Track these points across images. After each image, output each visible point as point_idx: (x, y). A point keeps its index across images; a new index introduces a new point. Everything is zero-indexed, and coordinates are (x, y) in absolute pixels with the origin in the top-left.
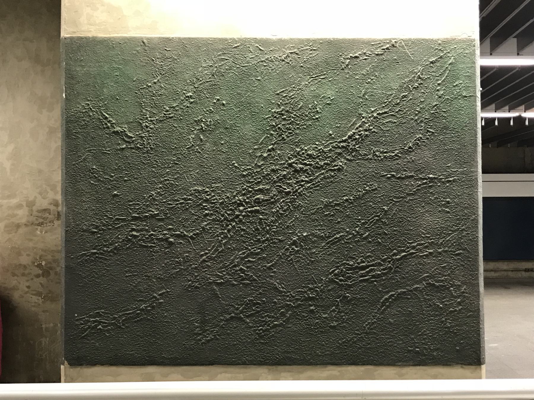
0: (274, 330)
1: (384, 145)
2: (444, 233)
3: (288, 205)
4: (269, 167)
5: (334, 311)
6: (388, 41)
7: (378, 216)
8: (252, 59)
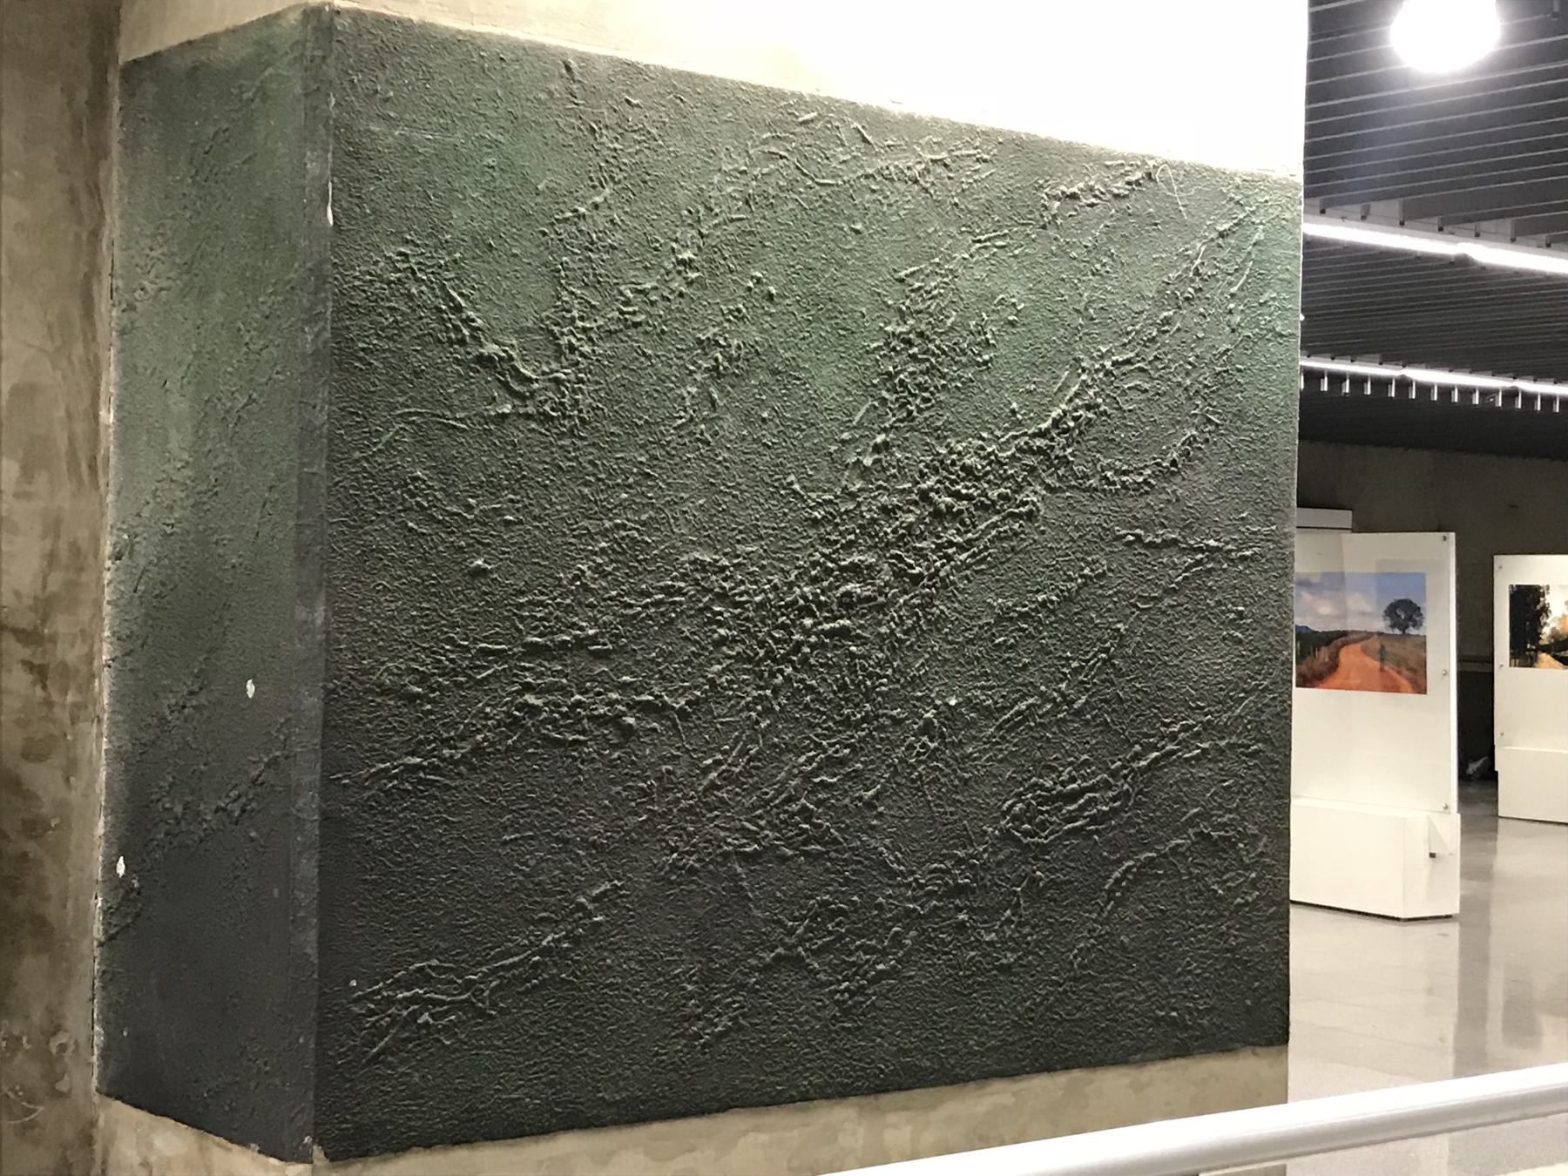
0: (876, 988)
4: (875, 498)
5: (1009, 921)
7: (1106, 651)
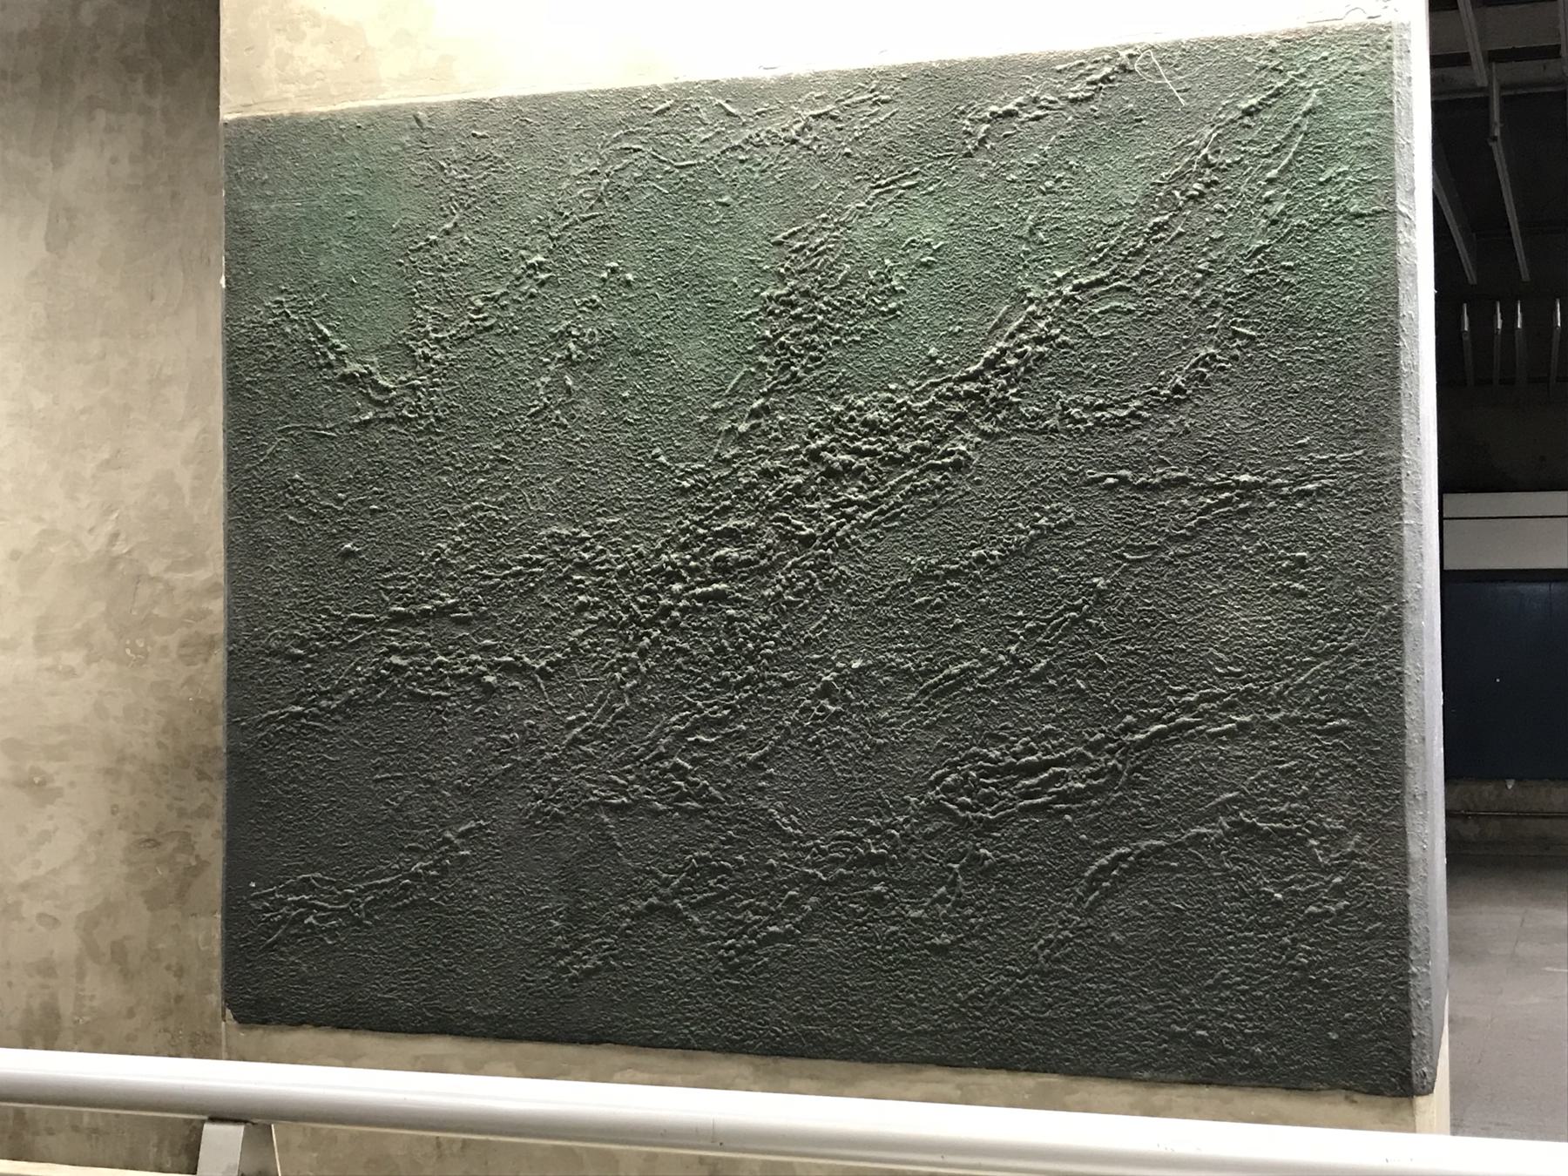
1: (1095, 386)
2: (1289, 663)
3: (809, 576)
4: (753, 463)
5: (942, 900)
6: (1107, 57)
7: (1078, 608)
8: (706, 145)
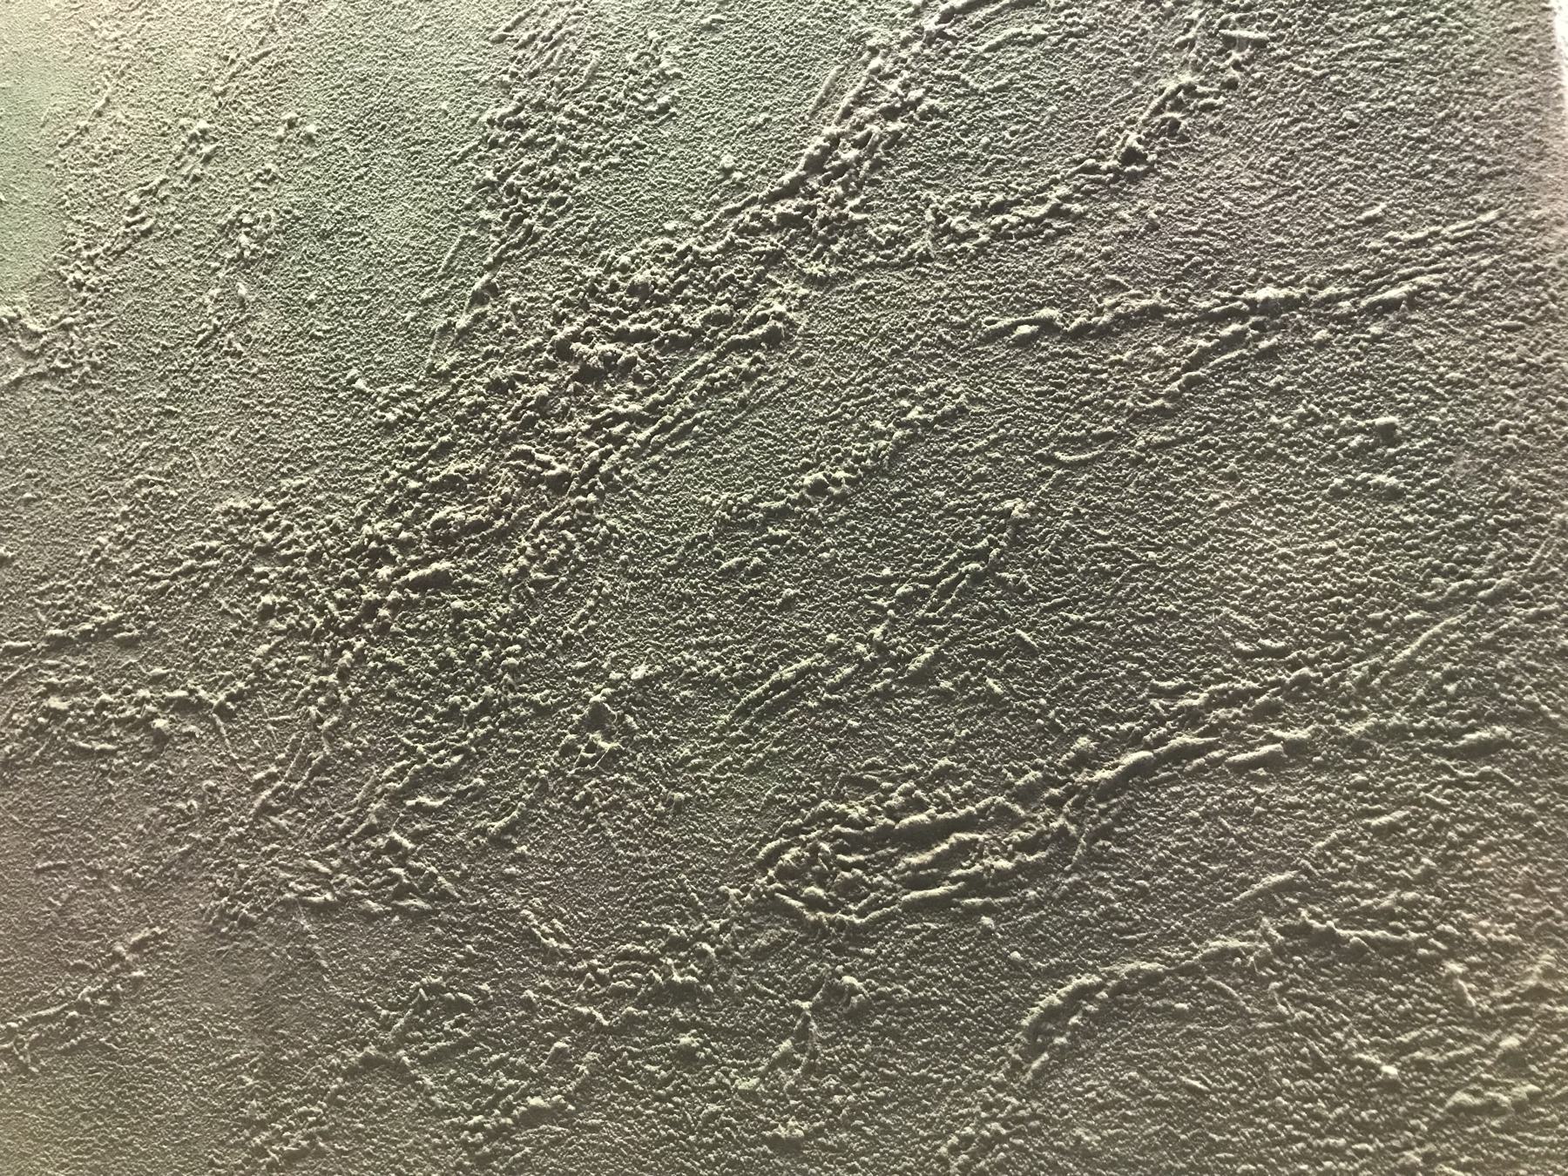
0: (530, 1133)
1: (988, 173)
2: (1377, 625)
3: (564, 538)
5: (787, 1061)
7: (981, 555)
